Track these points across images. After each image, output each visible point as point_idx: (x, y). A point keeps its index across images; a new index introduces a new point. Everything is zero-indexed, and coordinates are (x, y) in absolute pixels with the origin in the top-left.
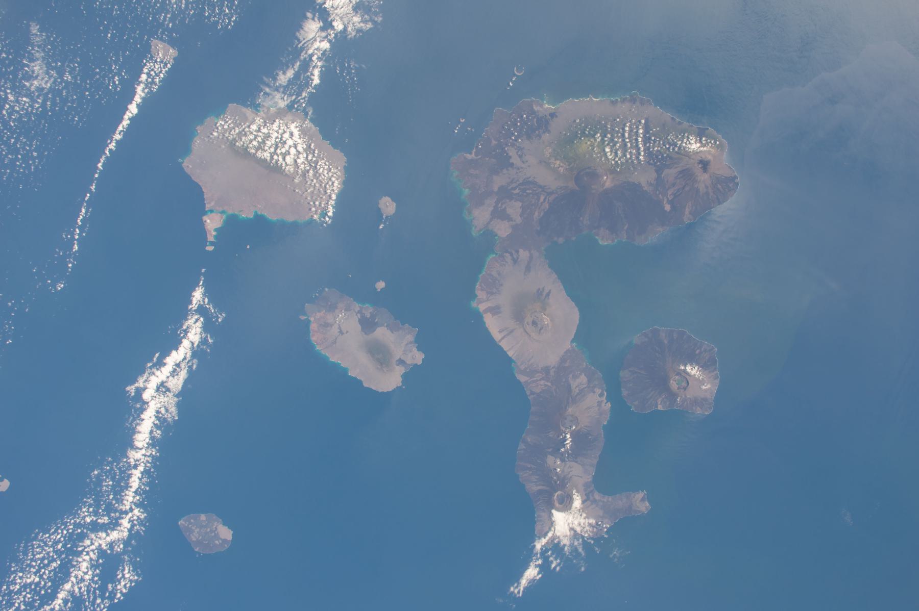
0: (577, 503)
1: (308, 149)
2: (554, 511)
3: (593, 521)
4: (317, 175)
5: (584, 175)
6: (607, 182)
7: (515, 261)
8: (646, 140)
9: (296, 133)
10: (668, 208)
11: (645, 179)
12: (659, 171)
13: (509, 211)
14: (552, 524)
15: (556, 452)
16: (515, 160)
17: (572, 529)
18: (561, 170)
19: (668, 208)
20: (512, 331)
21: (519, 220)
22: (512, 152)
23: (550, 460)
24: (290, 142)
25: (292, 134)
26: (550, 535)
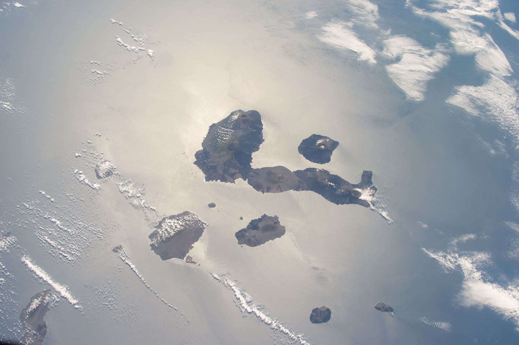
0: (359, 190)
1: (178, 220)
2: (360, 198)
3: (369, 188)
4: (189, 221)
5: (230, 147)
6: (236, 142)
7: (252, 177)
8: (227, 128)
9: (170, 221)
10: (254, 130)
11: (240, 133)
12: (240, 129)
13: (233, 172)
14: (365, 201)
15: (335, 190)
16: (214, 164)
17: (370, 195)
18: (225, 153)
19: (254, 130)
20: (280, 187)
21: (237, 171)
22: (211, 164)
23: (337, 192)
24: (172, 224)
25: (170, 222)
26: (370, 203)
